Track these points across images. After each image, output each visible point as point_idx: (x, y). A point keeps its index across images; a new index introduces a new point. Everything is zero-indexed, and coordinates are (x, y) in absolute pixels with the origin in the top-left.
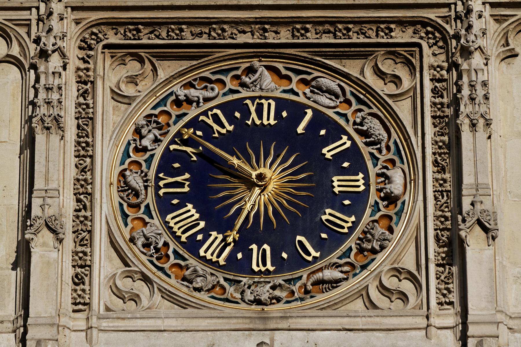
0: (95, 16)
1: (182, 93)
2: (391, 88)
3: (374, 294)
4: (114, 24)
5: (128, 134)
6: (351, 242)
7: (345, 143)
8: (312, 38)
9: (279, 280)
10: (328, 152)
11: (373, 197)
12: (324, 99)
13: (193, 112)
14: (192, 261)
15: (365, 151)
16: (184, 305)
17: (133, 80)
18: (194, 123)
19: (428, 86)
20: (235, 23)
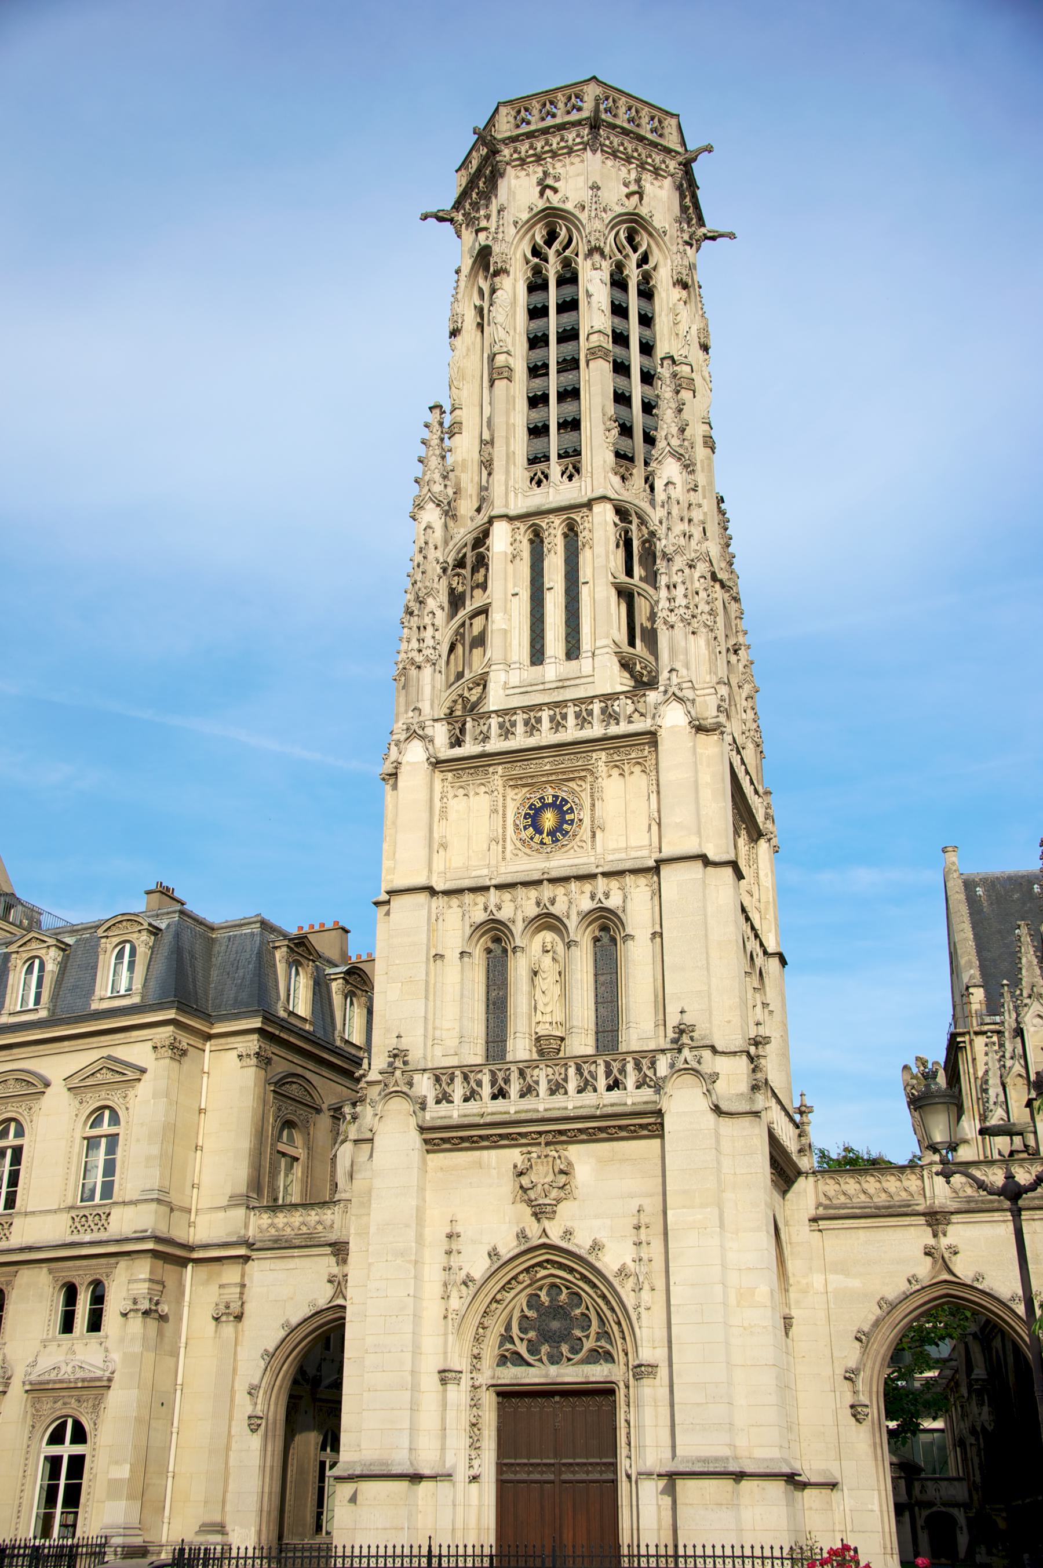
0: (506, 778)
1: (528, 796)
2: (581, 789)
3: (575, 847)
4: (511, 779)
5: (516, 810)
6: (571, 833)
7: (569, 805)
8: (560, 777)
9: (553, 846)
10: (565, 809)
11: (576, 820)
12: (564, 794)
13: (532, 801)
14: (532, 843)
15: (574, 807)
16: (529, 856)
17: (516, 794)
18: (532, 804)
19: (589, 787)
20: (541, 775)
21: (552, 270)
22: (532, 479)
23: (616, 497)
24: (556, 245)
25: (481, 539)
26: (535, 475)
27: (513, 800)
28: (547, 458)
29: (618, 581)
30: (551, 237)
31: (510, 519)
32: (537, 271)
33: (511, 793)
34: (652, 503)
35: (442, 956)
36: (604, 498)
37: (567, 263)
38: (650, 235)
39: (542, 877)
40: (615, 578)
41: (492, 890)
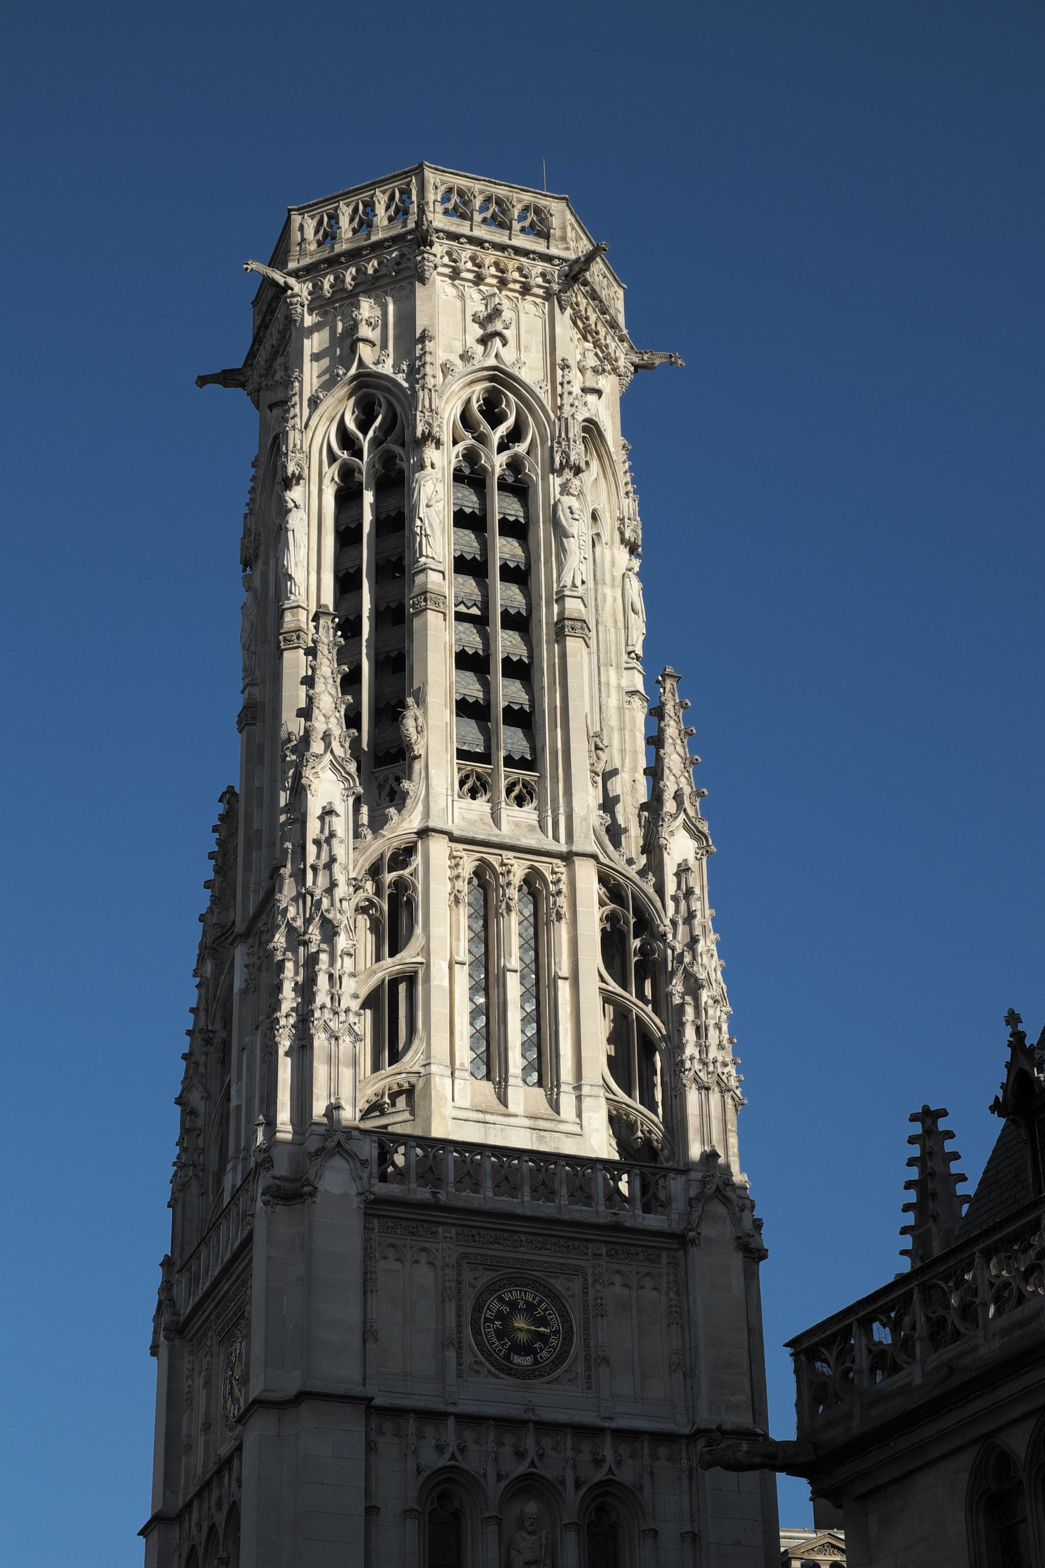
21: (497, 463)
22: (462, 783)
23: (606, 861)
24: (502, 429)
25: (403, 856)
26: (467, 777)
27: (470, 1285)
28: (485, 757)
29: (610, 988)
30: (493, 413)
31: (453, 839)
32: (471, 456)
33: (468, 1275)
34: (660, 889)
35: (379, 1509)
36: (594, 857)
37: (515, 465)
38: (600, 457)
39: (526, 1417)
40: (603, 980)
41: (452, 1419)
